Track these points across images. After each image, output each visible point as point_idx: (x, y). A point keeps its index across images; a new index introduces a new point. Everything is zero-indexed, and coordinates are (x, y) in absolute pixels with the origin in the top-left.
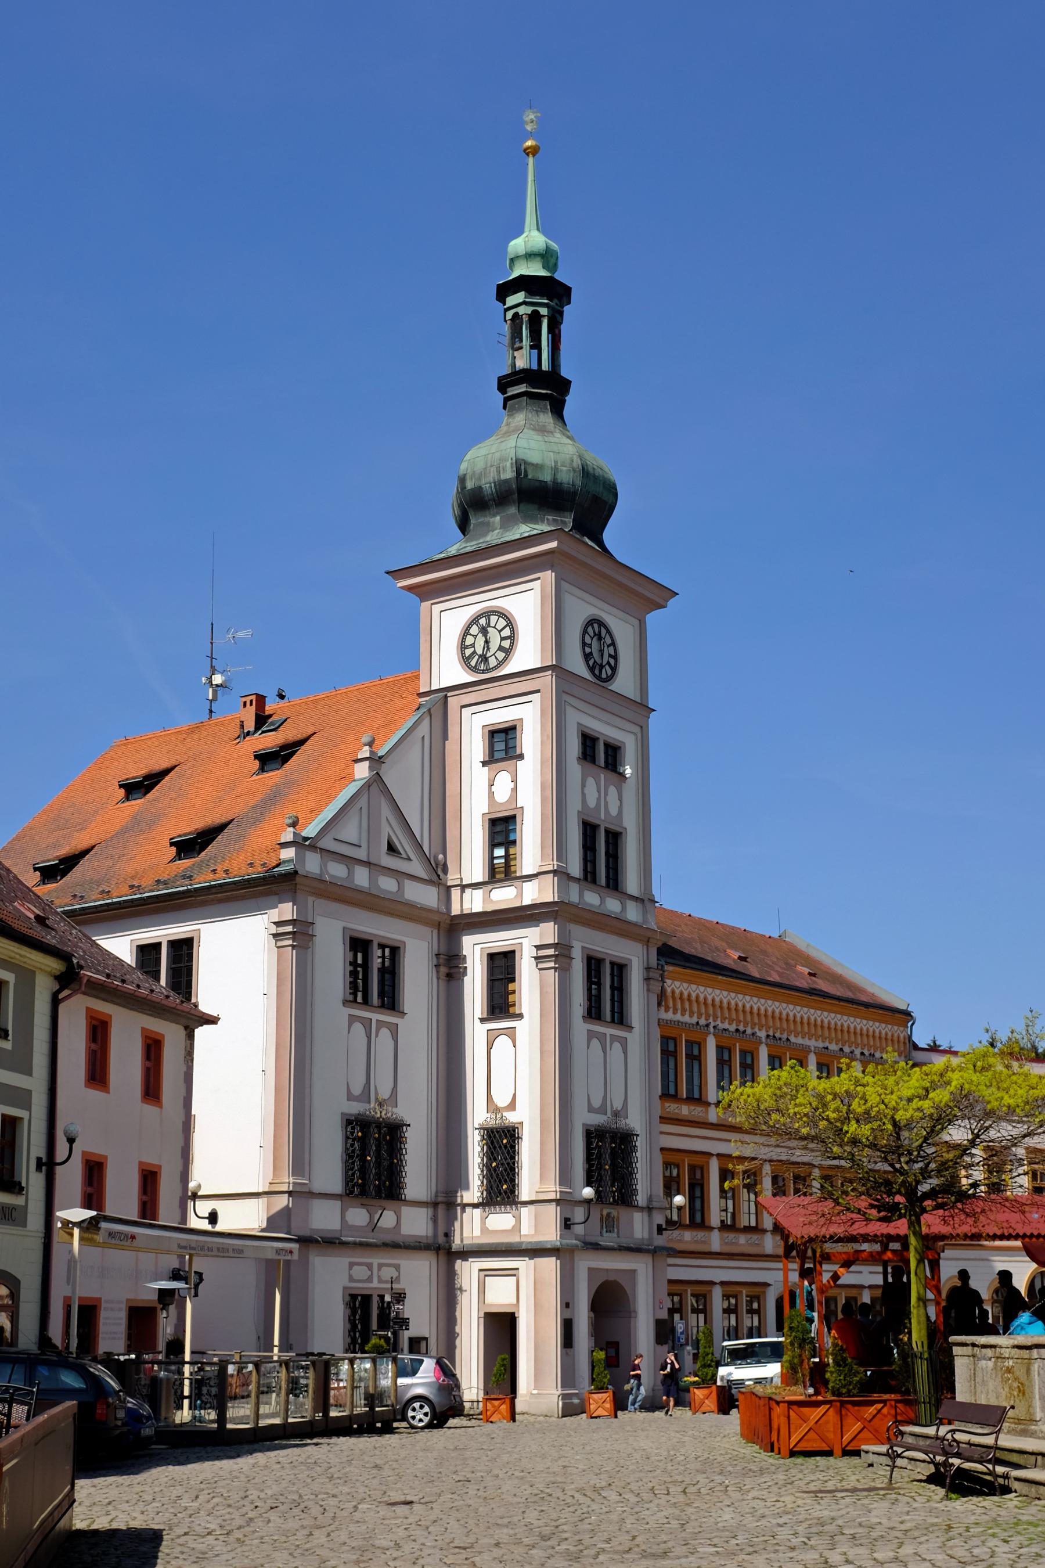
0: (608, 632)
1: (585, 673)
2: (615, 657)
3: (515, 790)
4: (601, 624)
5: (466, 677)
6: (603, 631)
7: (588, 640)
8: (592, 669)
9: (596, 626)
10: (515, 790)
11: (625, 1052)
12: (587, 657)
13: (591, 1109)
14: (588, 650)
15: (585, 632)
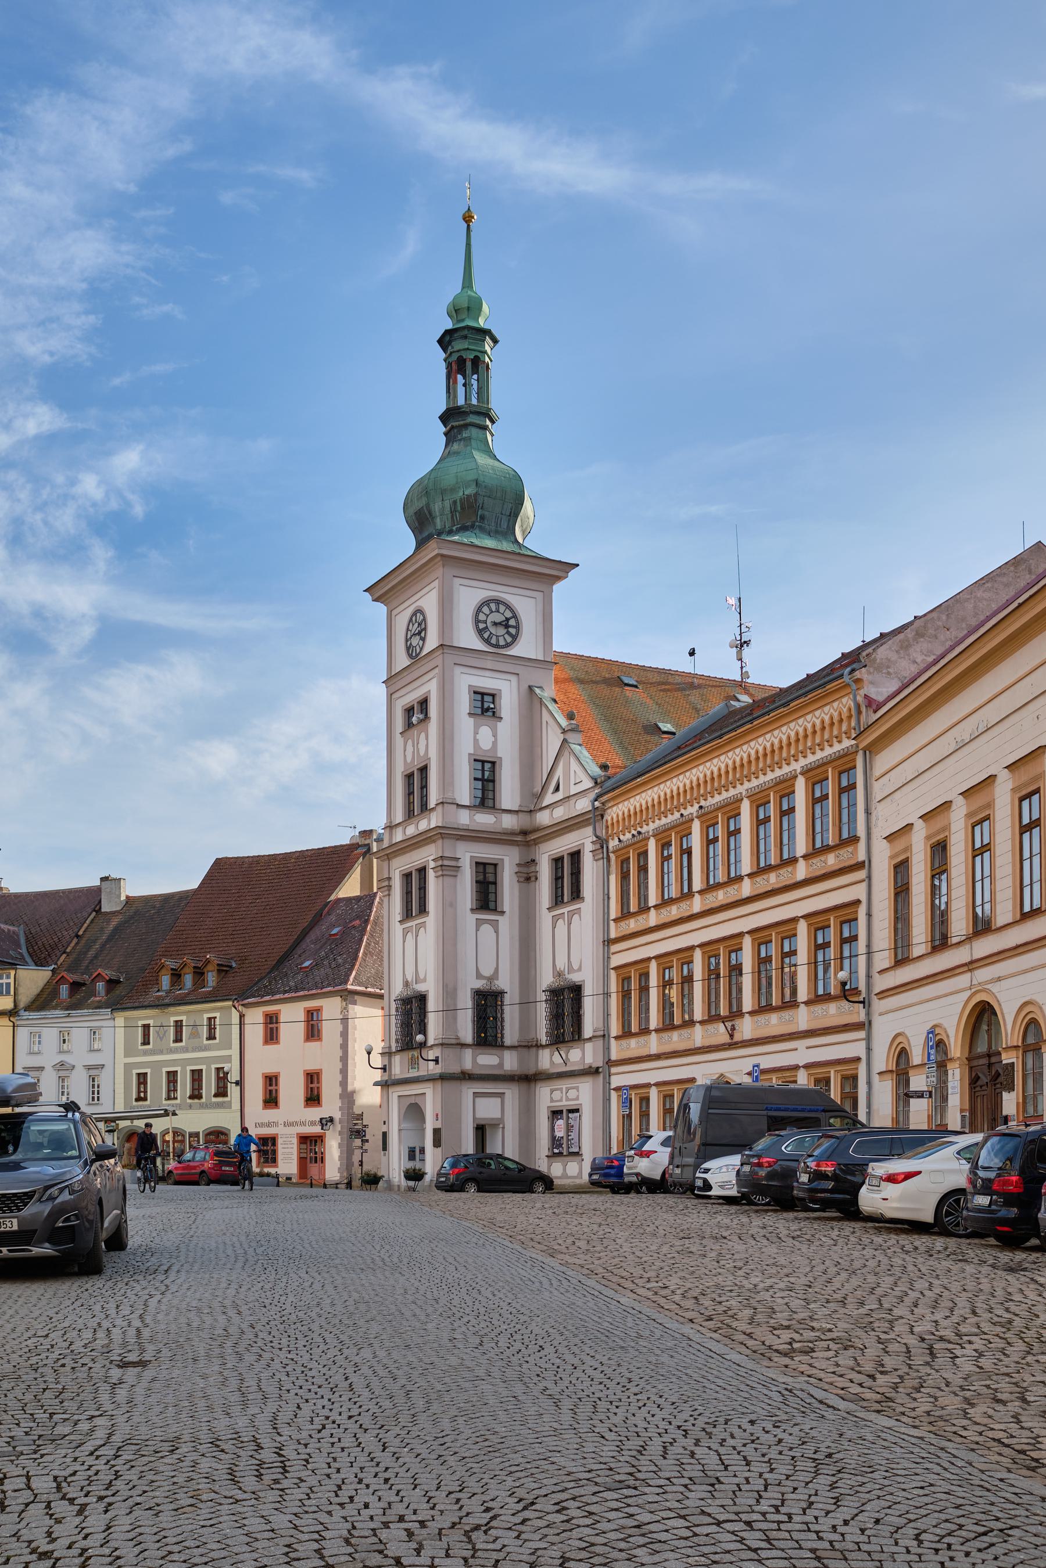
0: (508, 607)
1: (480, 646)
2: (517, 627)
3: (427, 746)
4: (498, 602)
5: (407, 662)
6: (502, 608)
7: (482, 617)
8: (487, 641)
9: (493, 606)
10: (427, 746)
11: (497, 932)
12: (480, 632)
13: (479, 976)
14: (482, 626)
15: (479, 610)
